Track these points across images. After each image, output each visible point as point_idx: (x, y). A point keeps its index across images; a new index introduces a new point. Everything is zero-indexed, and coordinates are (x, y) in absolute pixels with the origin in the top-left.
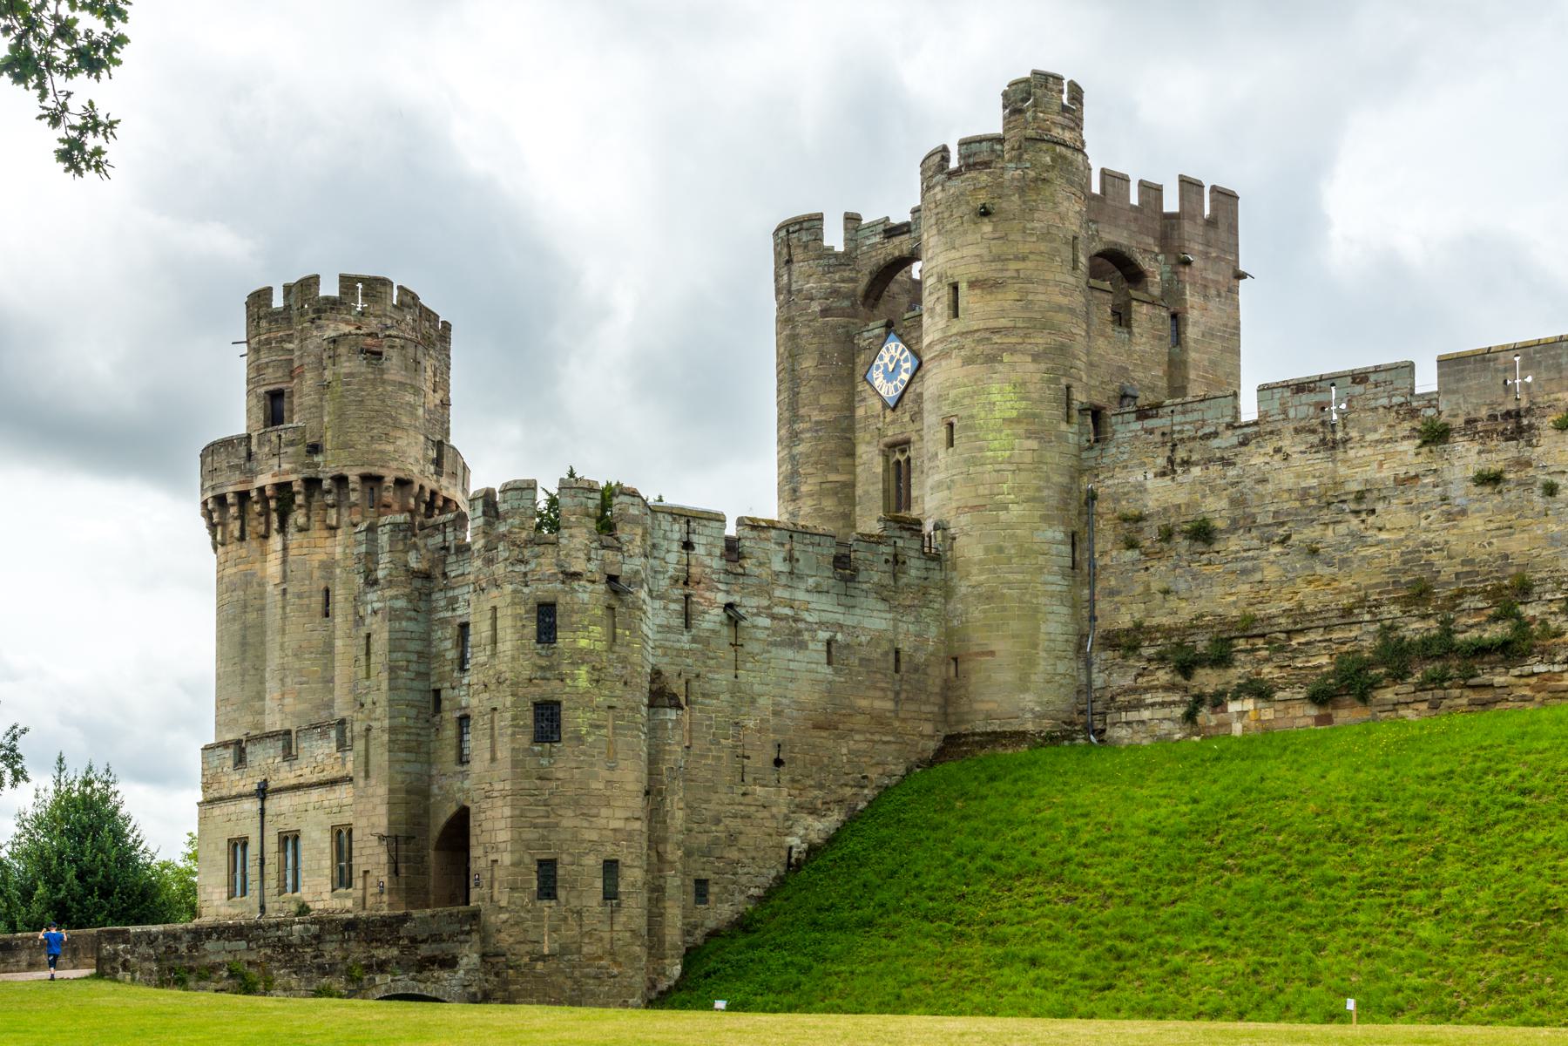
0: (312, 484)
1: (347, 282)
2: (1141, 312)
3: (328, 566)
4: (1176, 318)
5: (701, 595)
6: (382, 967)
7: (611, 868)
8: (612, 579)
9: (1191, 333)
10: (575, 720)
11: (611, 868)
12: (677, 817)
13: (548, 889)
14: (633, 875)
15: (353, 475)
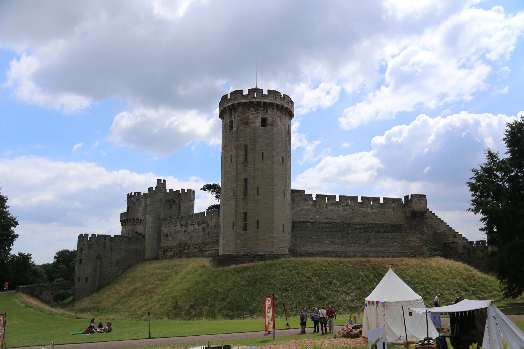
0: (127, 219)
1: (135, 193)
2: (174, 206)
3: (129, 230)
4: (180, 206)
5: (107, 245)
6: (60, 289)
7: (87, 278)
8: (90, 245)
9: (181, 208)
10: (83, 261)
11: (87, 278)
12: (98, 271)
13: (79, 281)
14: (90, 279)
15: (131, 218)
